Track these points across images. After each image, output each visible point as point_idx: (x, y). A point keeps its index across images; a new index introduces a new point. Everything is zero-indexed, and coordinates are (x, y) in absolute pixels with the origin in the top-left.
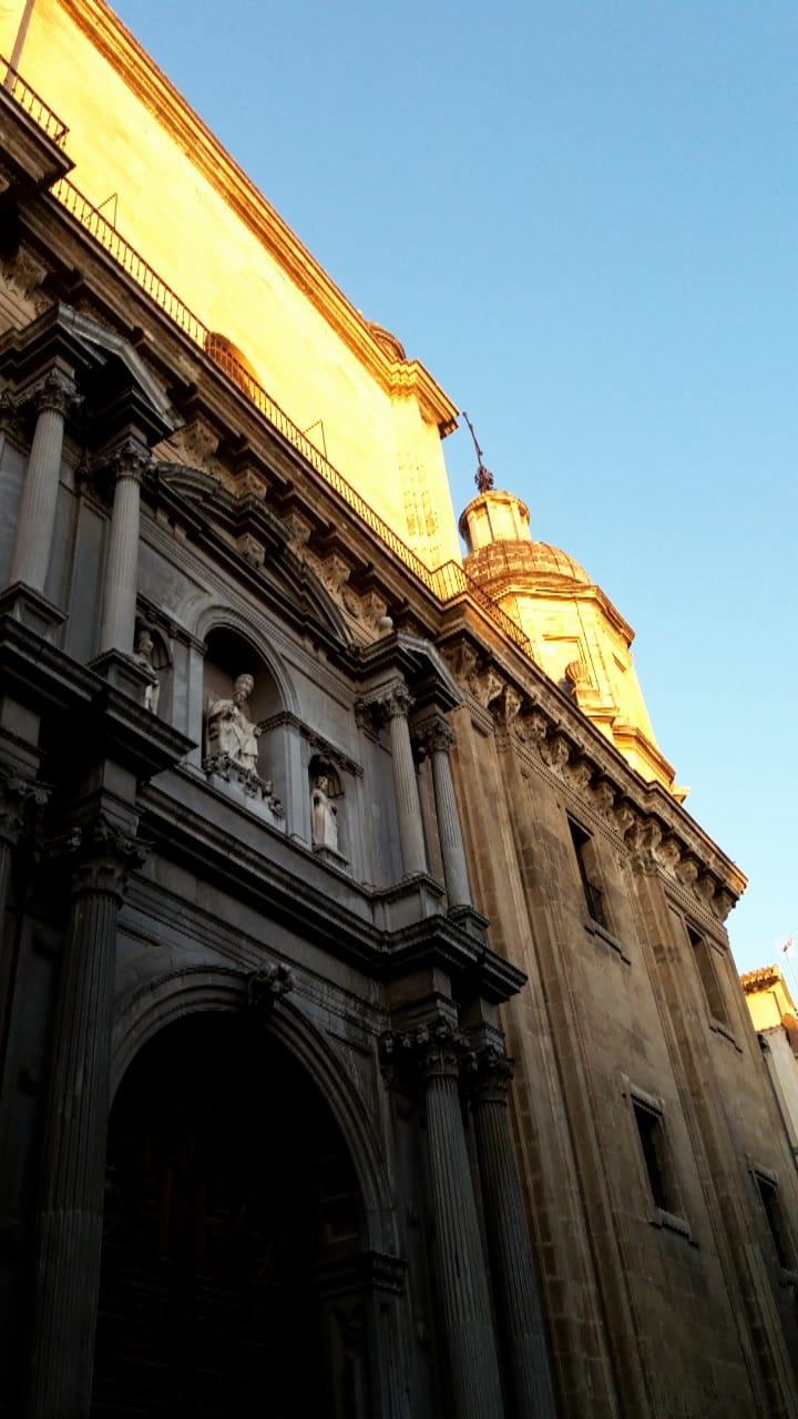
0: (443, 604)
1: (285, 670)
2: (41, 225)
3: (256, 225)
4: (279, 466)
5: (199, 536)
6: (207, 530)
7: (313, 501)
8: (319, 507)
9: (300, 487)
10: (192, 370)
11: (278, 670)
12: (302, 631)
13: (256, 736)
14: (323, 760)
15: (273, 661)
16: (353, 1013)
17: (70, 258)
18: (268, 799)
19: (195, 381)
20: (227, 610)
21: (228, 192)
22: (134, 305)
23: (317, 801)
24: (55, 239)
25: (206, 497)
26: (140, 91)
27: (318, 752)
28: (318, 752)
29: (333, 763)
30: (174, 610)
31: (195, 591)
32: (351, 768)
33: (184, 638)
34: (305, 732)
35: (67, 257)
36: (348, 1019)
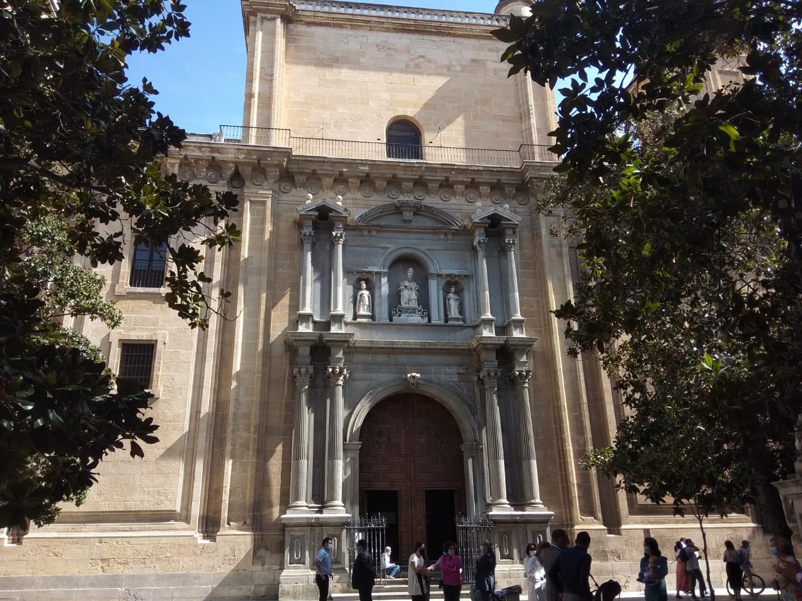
0: (521, 168)
1: (428, 256)
2: (296, 166)
3: (411, 30)
4: (414, 173)
5: (380, 229)
6: (381, 227)
7: (435, 174)
8: (438, 174)
9: (426, 174)
10: (364, 168)
11: (425, 258)
12: (437, 234)
13: (418, 291)
14: (452, 280)
15: (422, 255)
16: (461, 371)
17: (309, 168)
18: (419, 313)
19: (367, 171)
20: (397, 249)
21: (394, 28)
22: (336, 165)
23: (449, 299)
24: (304, 167)
25: (381, 212)
26: (341, 26)
27: (448, 279)
28: (448, 279)
29: (457, 279)
30: (374, 265)
31: (384, 250)
32: (466, 276)
33: (379, 274)
34: (439, 276)
35: (308, 169)
36: (459, 374)
